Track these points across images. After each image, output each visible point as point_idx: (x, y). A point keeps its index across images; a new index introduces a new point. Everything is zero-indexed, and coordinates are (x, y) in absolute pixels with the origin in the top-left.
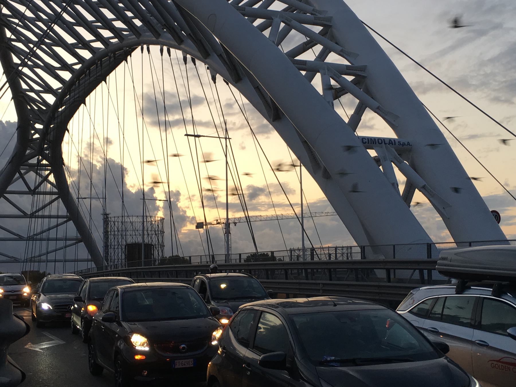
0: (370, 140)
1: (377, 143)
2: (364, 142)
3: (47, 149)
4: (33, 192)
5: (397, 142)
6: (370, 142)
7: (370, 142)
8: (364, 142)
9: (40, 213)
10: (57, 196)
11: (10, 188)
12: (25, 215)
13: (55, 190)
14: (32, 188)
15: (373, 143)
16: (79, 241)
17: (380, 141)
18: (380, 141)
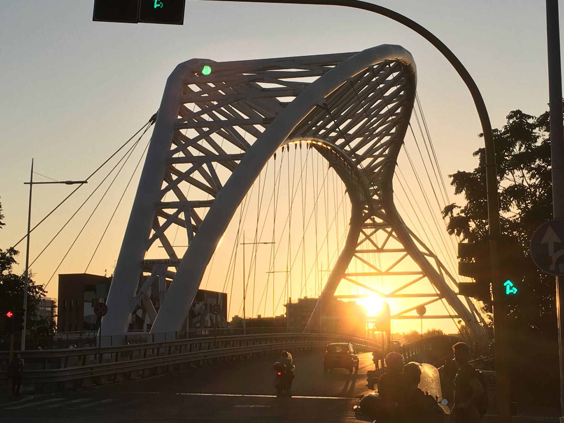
0: (151, 261)
1: (156, 262)
2: (147, 263)
3: (381, 208)
4: (380, 250)
5: (170, 262)
6: (151, 263)
7: (151, 263)
8: (147, 263)
9: (373, 271)
10: (406, 253)
11: (358, 248)
12: (380, 273)
13: (401, 246)
14: (380, 247)
15: (154, 264)
17: (158, 263)
18: (158, 263)
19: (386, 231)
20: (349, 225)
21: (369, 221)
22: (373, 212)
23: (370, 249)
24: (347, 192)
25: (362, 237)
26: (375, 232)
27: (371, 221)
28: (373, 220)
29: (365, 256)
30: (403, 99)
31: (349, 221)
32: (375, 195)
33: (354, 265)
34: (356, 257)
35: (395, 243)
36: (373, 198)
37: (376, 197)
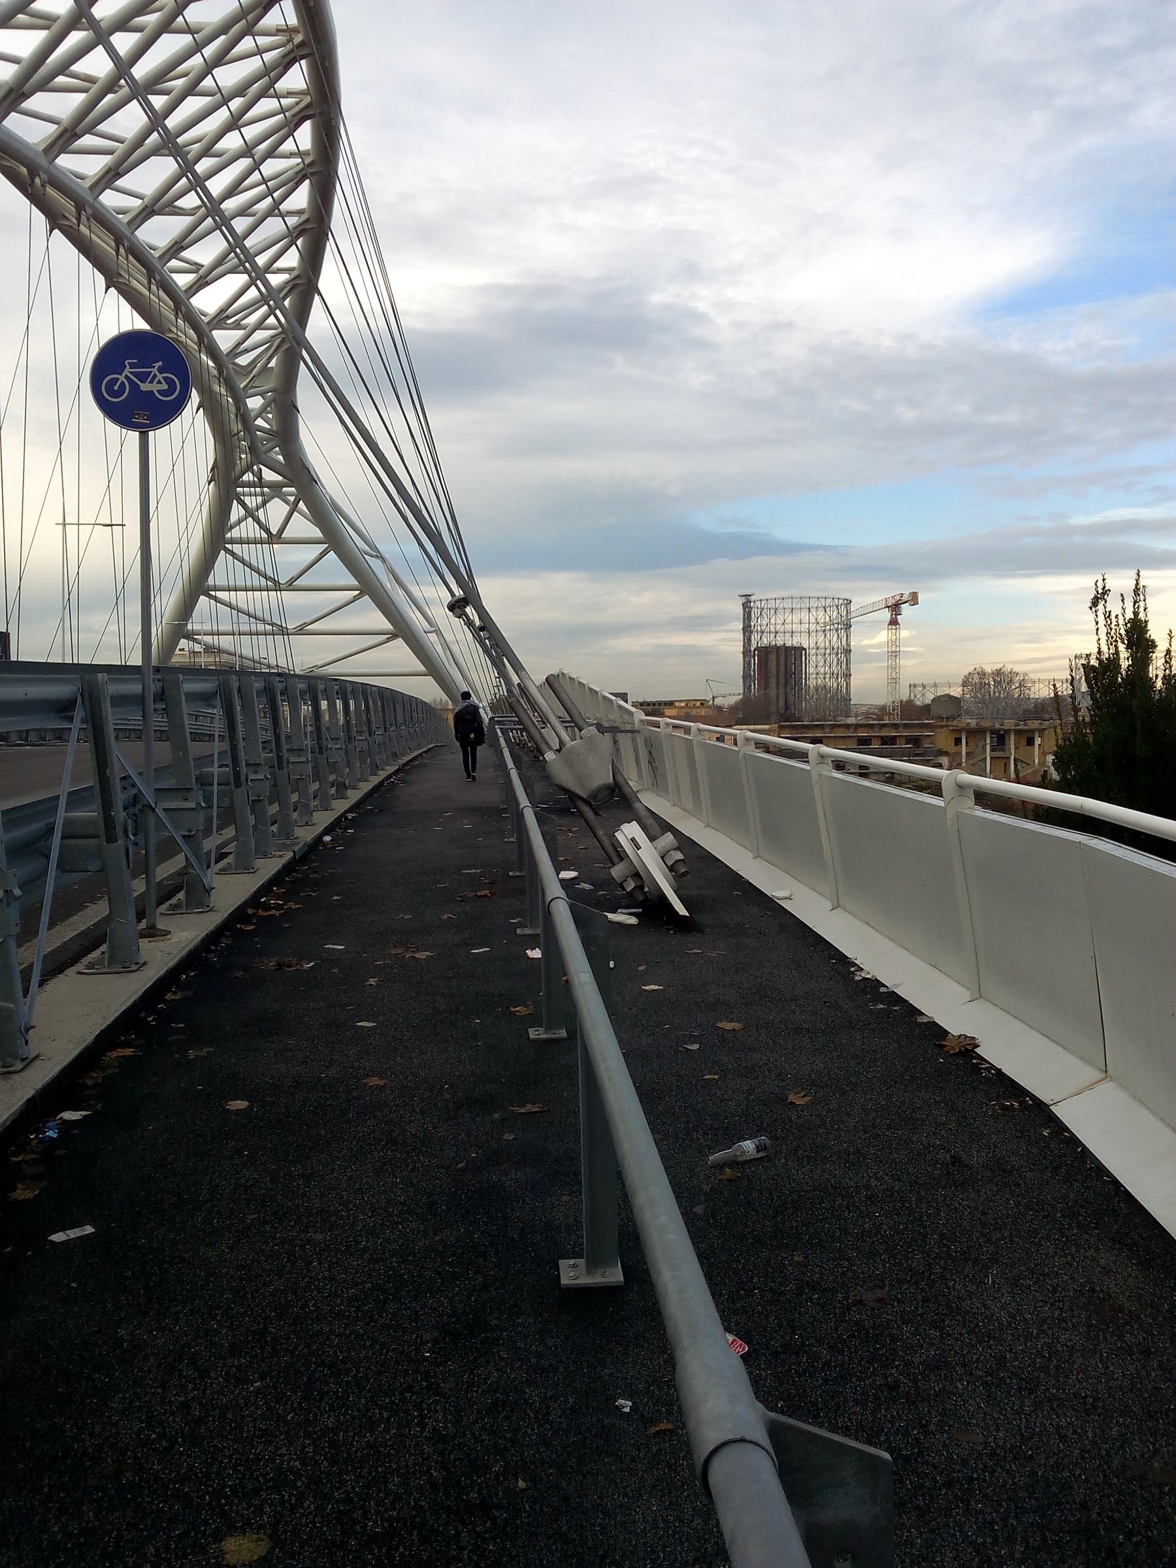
4: (274, 538)
9: (257, 580)
11: (228, 535)
13: (316, 533)
14: (274, 533)
16: (394, 636)
19: (287, 502)
20: (209, 485)
21: (248, 477)
22: (257, 456)
23: (251, 535)
24: (201, 409)
25: (236, 512)
26: (264, 503)
27: (251, 475)
28: (259, 475)
29: (236, 548)
30: (308, 160)
31: (205, 475)
32: (259, 419)
33: (223, 570)
34: (227, 551)
35: (302, 526)
36: (256, 423)
37: (260, 422)
